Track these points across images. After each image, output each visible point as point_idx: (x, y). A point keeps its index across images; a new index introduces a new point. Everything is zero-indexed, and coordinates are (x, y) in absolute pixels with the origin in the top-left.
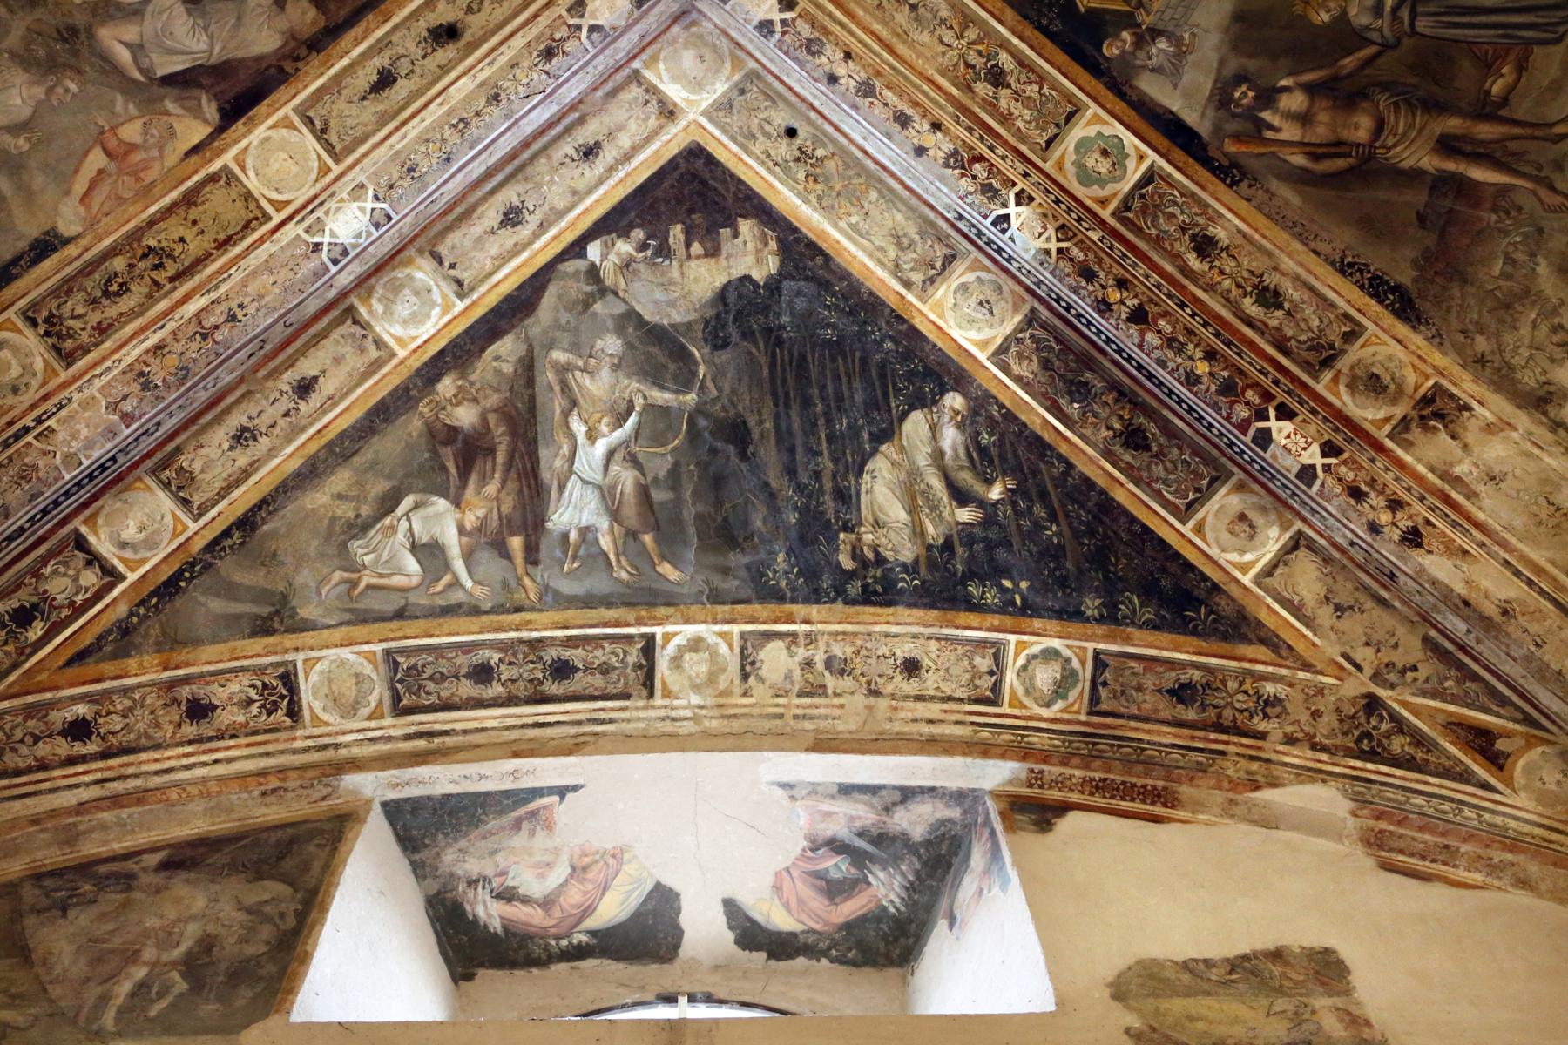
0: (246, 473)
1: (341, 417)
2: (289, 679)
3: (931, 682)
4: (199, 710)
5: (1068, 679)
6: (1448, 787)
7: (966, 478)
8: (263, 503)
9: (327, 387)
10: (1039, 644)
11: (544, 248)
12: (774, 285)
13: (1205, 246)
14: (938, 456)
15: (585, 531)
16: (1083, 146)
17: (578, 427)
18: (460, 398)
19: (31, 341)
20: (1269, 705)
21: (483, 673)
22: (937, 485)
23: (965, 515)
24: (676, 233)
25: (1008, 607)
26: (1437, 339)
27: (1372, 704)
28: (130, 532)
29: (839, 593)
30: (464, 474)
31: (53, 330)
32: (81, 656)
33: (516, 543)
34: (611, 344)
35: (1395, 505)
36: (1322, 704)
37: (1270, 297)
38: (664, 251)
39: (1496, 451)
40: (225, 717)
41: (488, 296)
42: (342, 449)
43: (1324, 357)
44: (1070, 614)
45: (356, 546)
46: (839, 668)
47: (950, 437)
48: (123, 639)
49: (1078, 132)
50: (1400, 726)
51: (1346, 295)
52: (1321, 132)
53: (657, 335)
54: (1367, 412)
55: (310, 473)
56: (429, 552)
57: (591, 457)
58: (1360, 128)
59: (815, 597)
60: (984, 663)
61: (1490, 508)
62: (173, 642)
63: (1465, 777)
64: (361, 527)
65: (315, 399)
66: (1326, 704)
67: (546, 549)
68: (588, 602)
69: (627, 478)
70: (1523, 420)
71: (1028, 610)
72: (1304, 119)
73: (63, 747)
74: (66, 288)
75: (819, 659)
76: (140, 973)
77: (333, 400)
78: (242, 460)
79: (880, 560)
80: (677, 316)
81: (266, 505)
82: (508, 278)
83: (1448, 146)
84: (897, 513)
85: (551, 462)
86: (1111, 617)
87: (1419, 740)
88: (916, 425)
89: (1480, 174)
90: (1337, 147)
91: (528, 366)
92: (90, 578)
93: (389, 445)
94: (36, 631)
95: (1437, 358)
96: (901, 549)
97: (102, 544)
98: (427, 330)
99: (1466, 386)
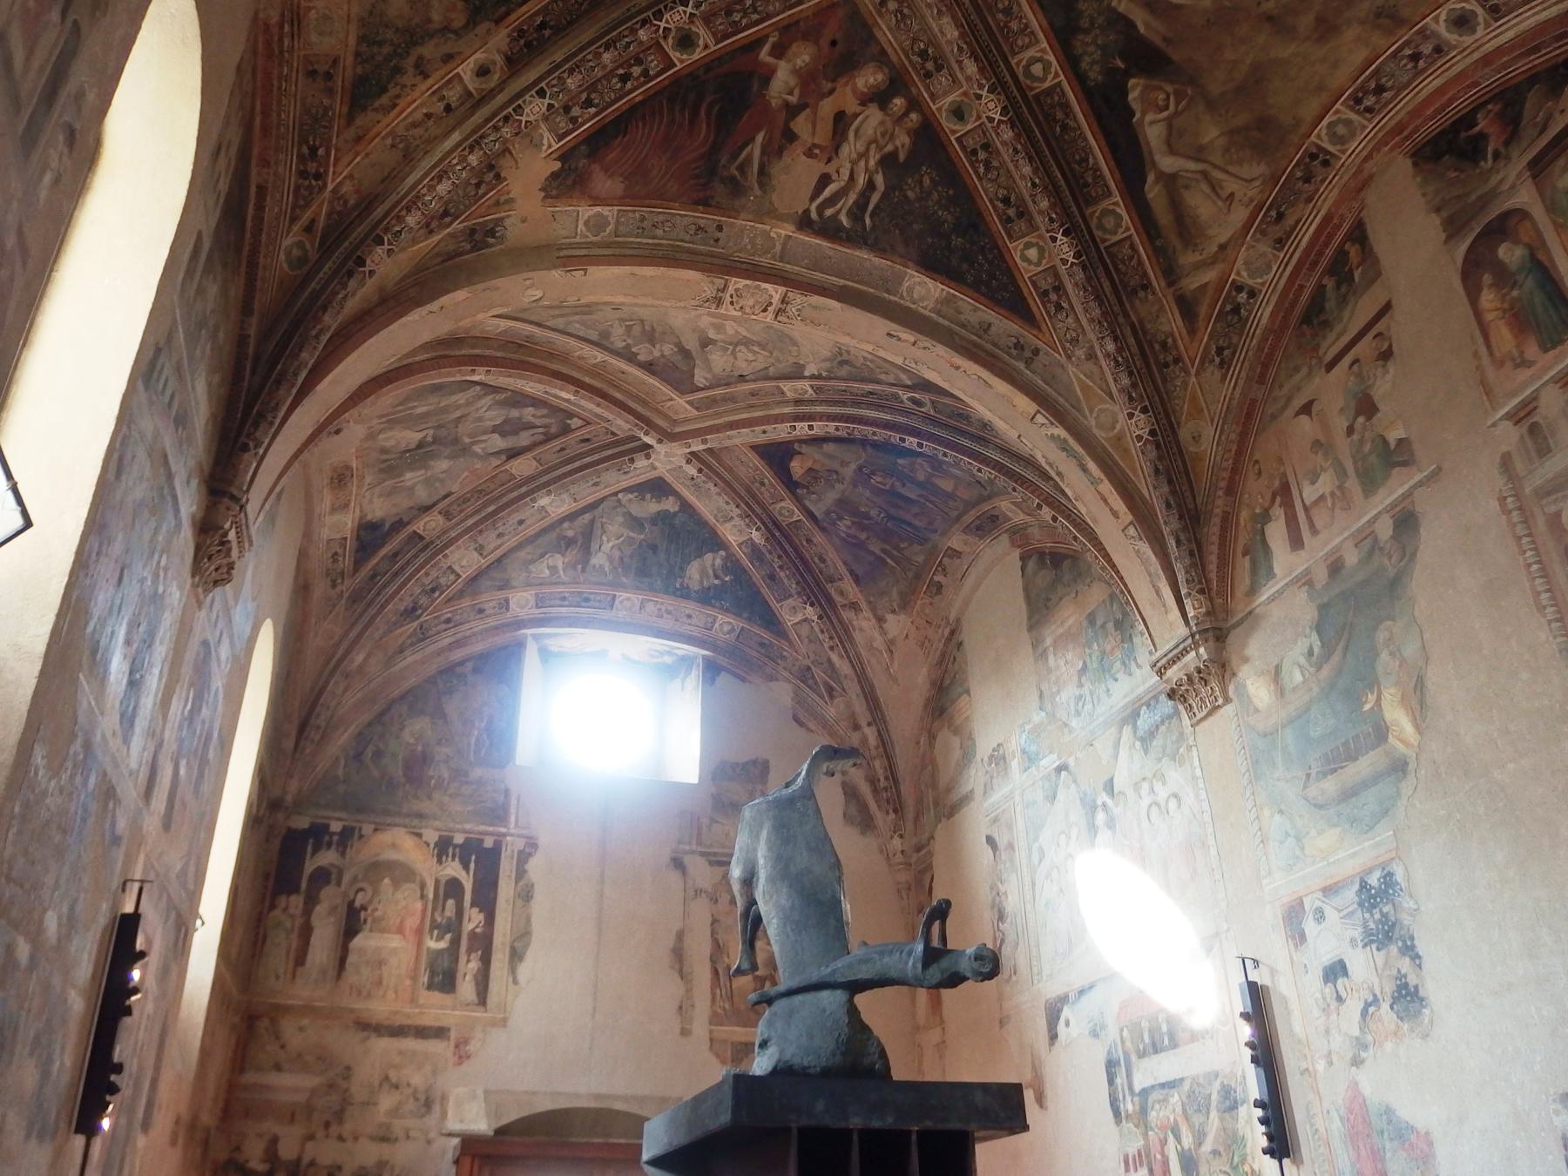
0: (500, 546)
1: (531, 531)
2: (507, 601)
3: (694, 621)
4: (481, 611)
5: (733, 630)
6: (817, 699)
7: (720, 573)
8: (504, 555)
9: (528, 523)
10: (727, 620)
11: (606, 492)
12: (675, 514)
13: (809, 541)
14: (713, 565)
15: (601, 566)
16: (781, 508)
17: (604, 538)
18: (570, 528)
19: (441, 519)
20: (783, 657)
21: (564, 599)
22: (711, 572)
23: (716, 582)
24: (648, 496)
25: (721, 608)
26: (861, 591)
27: (809, 668)
28: (464, 563)
29: (674, 594)
30: (567, 549)
31: (447, 514)
32: (449, 600)
33: (580, 567)
34: (620, 519)
35: (831, 638)
36: (797, 663)
37: (823, 560)
38: (643, 499)
39: (864, 624)
40: (487, 612)
41: (582, 504)
42: (531, 540)
43: (831, 580)
44: (738, 615)
45: (532, 568)
46: (669, 613)
47: (718, 561)
48: (461, 594)
49: (783, 504)
50: (813, 677)
51: (843, 570)
52: (853, 531)
53: (635, 519)
54: (838, 598)
55: (519, 547)
56: (553, 569)
57: (607, 547)
58: (863, 536)
59: (666, 592)
60: (710, 620)
61: (857, 636)
62: (476, 594)
63: (822, 697)
64: (532, 562)
65: (523, 526)
66: (797, 663)
67: (589, 569)
68: (598, 584)
69: (617, 554)
70: (874, 621)
71: (727, 610)
72: (849, 528)
73: (444, 626)
74: (451, 504)
75: (663, 608)
76: (476, 732)
77: (530, 526)
78: (499, 542)
79: (688, 587)
80: (643, 515)
81: (504, 555)
82: (590, 499)
83: (883, 550)
84: (697, 577)
85: (594, 546)
86: (749, 620)
87: (816, 683)
88: (709, 557)
89: (889, 561)
90: (855, 537)
91: (592, 521)
92: (452, 577)
93: (544, 540)
94: (437, 594)
95: (859, 595)
96: (695, 586)
97: (456, 568)
98: (563, 509)
99: (864, 605)
